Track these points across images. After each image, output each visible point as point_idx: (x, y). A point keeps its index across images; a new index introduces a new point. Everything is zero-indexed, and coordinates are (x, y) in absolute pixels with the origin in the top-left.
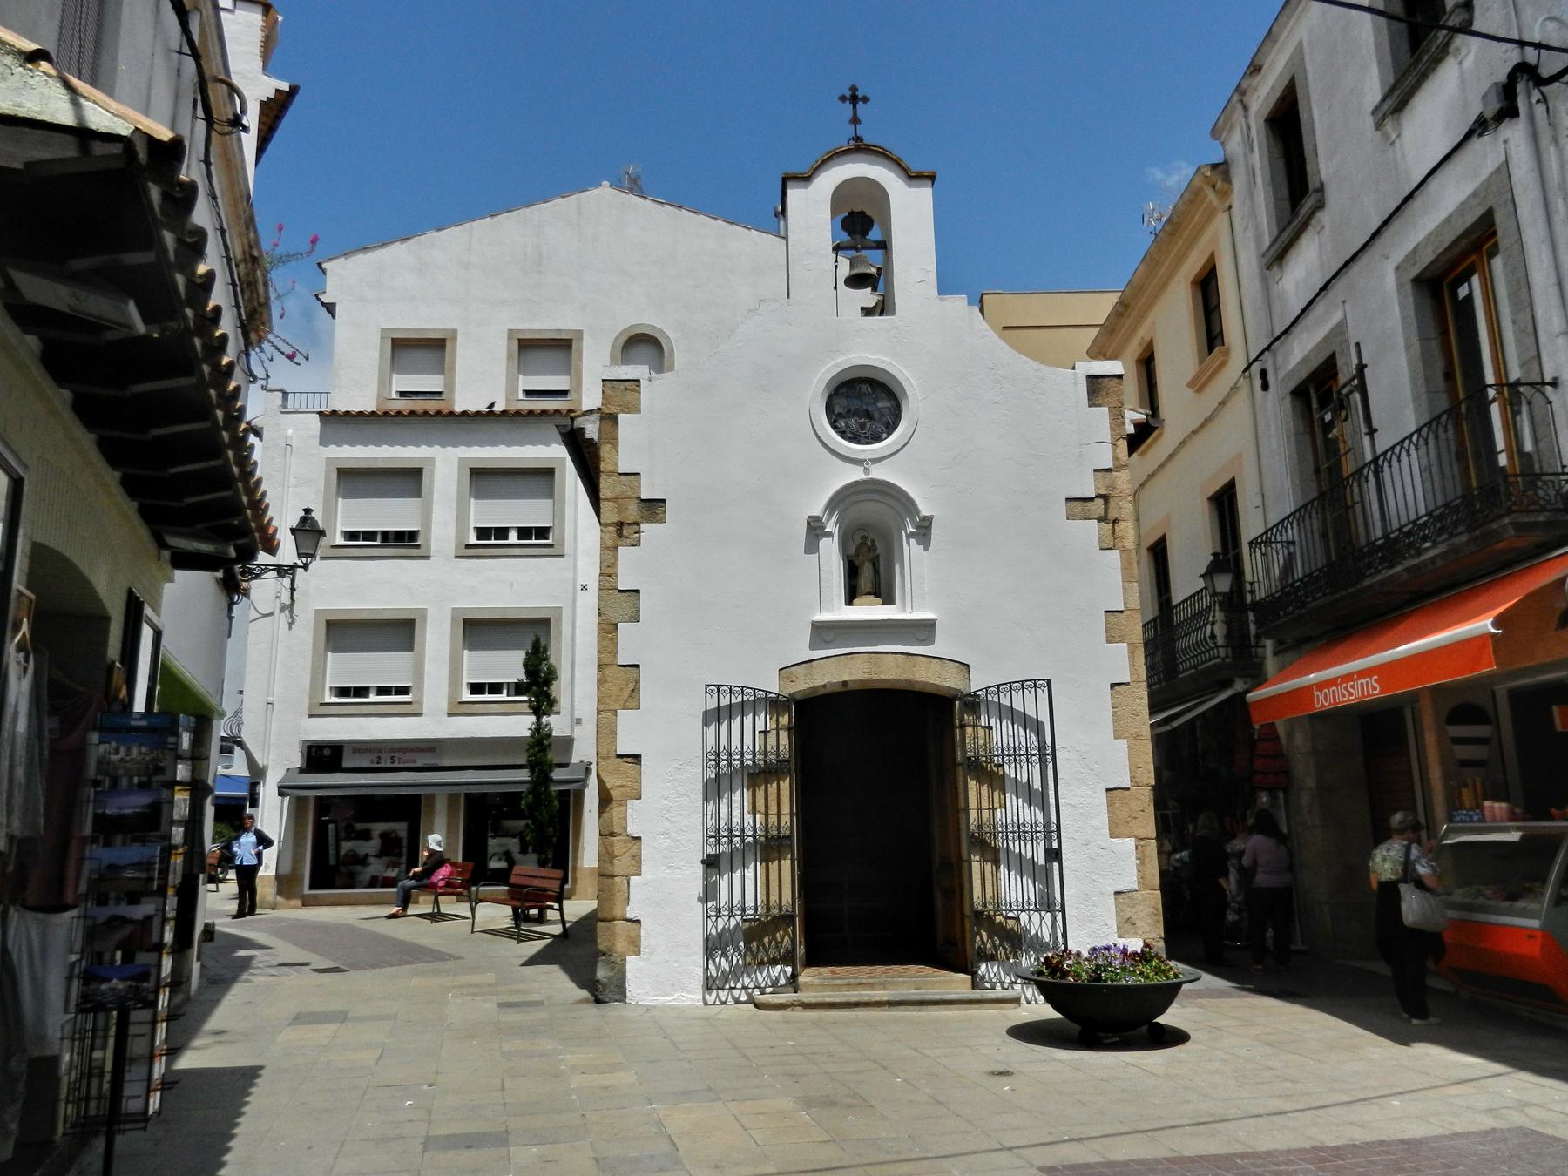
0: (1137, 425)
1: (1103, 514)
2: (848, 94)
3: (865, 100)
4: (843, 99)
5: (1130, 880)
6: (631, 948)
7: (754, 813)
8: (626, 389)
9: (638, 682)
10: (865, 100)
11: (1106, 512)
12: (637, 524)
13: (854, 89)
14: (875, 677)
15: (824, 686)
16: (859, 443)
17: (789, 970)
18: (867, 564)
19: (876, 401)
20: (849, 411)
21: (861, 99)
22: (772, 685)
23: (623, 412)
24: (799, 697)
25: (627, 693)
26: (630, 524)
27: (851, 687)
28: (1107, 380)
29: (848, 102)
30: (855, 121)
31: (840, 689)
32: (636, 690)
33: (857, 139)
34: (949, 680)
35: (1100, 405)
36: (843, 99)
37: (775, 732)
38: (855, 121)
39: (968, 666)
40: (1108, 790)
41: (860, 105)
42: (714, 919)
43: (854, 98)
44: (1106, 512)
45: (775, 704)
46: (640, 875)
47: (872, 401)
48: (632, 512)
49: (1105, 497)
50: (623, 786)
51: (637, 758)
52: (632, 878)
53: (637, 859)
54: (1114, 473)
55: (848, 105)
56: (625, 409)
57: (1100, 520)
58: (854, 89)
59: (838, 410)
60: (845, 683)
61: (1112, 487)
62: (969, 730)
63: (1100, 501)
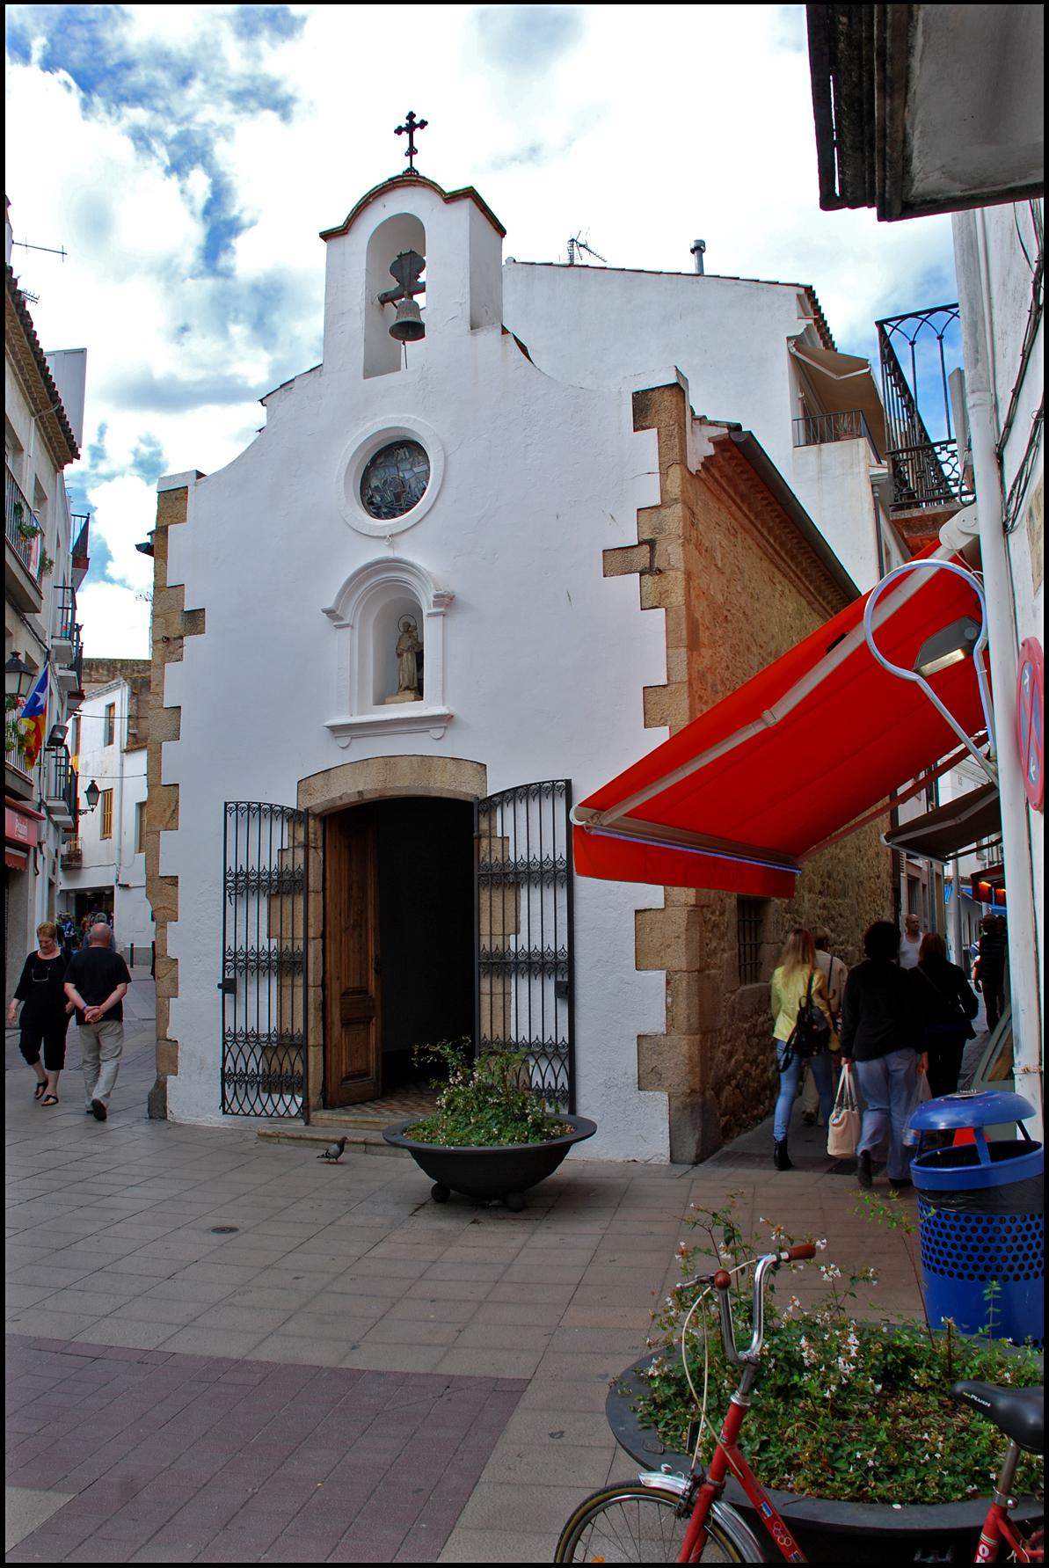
0: (719, 444)
1: (647, 565)
2: (404, 123)
3: (423, 124)
4: (399, 131)
5: (655, 1023)
6: (171, 1068)
7: (269, 937)
8: (176, 499)
9: (177, 802)
10: (423, 124)
11: (651, 561)
12: (181, 638)
13: (411, 116)
14: (390, 785)
15: (341, 798)
16: (394, 516)
17: (299, 1100)
18: (405, 655)
19: (413, 465)
20: (385, 482)
21: (416, 126)
22: (289, 799)
23: (172, 523)
24: (317, 811)
25: (169, 813)
26: (175, 639)
27: (368, 796)
28: (657, 393)
29: (404, 133)
30: (412, 151)
31: (356, 798)
32: (176, 811)
33: (411, 171)
34: (464, 787)
35: (649, 428)
36: (399, 131)
37: (291, 850)
38: (412, 151)
39: (485, 765)
40: (637, 912)
41: (417, 132)
42: (230, 1044)
43: (412, 126)
44: (651, 561)
45: (295, 817)
46: (177, 997)
47: (409, 467)
48: (178, 623)
49: (651, 543)
50: (164, 907)
51: (174, 880)
52: (171, 999)
53: (175, 980)
54: (664, 512)
55: (405, 135)
56: (175, 520)
57: (642, 573)
58: (411, 116)
59: (375, 482)
60: (360, 793)
61: (659, 529)
62: (485, 842)
63: (646, 548)
